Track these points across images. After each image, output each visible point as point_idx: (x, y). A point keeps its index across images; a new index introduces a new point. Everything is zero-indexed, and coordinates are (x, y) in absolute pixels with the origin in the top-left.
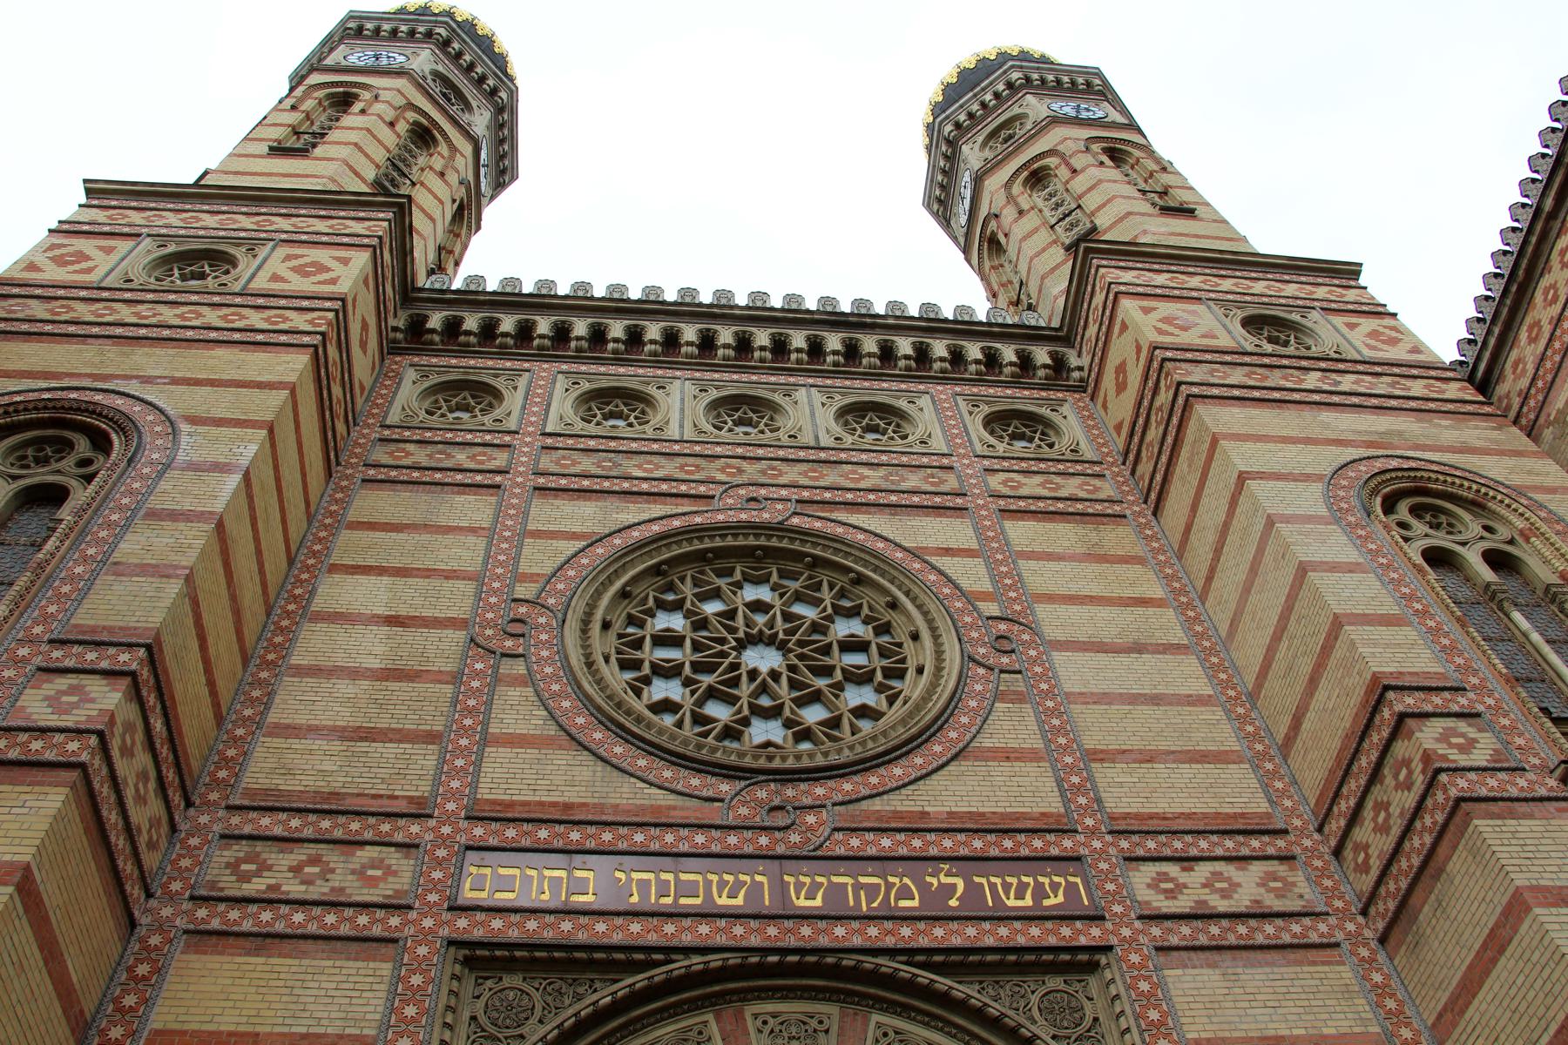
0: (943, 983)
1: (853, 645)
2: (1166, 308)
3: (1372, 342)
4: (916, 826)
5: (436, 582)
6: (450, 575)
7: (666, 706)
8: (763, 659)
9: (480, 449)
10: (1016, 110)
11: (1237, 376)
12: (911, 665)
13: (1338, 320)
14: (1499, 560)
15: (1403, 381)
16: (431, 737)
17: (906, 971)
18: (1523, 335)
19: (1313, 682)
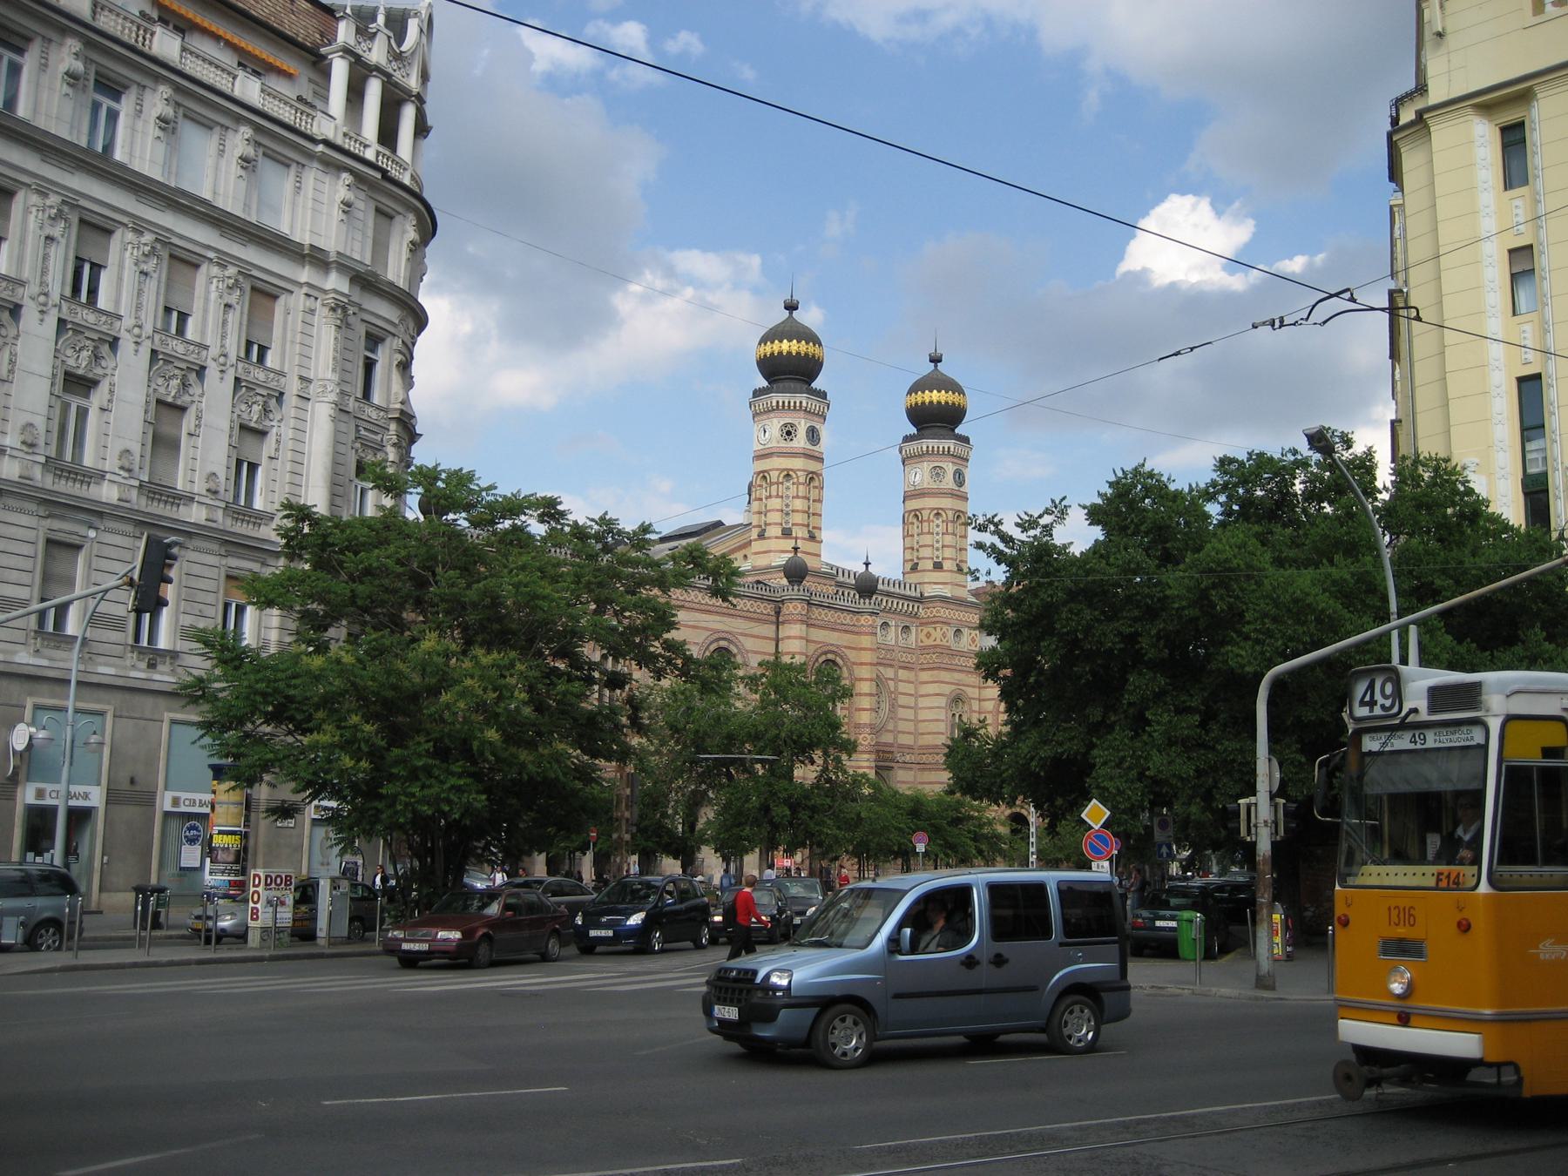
14: (960, 716)
19: (929, 733)
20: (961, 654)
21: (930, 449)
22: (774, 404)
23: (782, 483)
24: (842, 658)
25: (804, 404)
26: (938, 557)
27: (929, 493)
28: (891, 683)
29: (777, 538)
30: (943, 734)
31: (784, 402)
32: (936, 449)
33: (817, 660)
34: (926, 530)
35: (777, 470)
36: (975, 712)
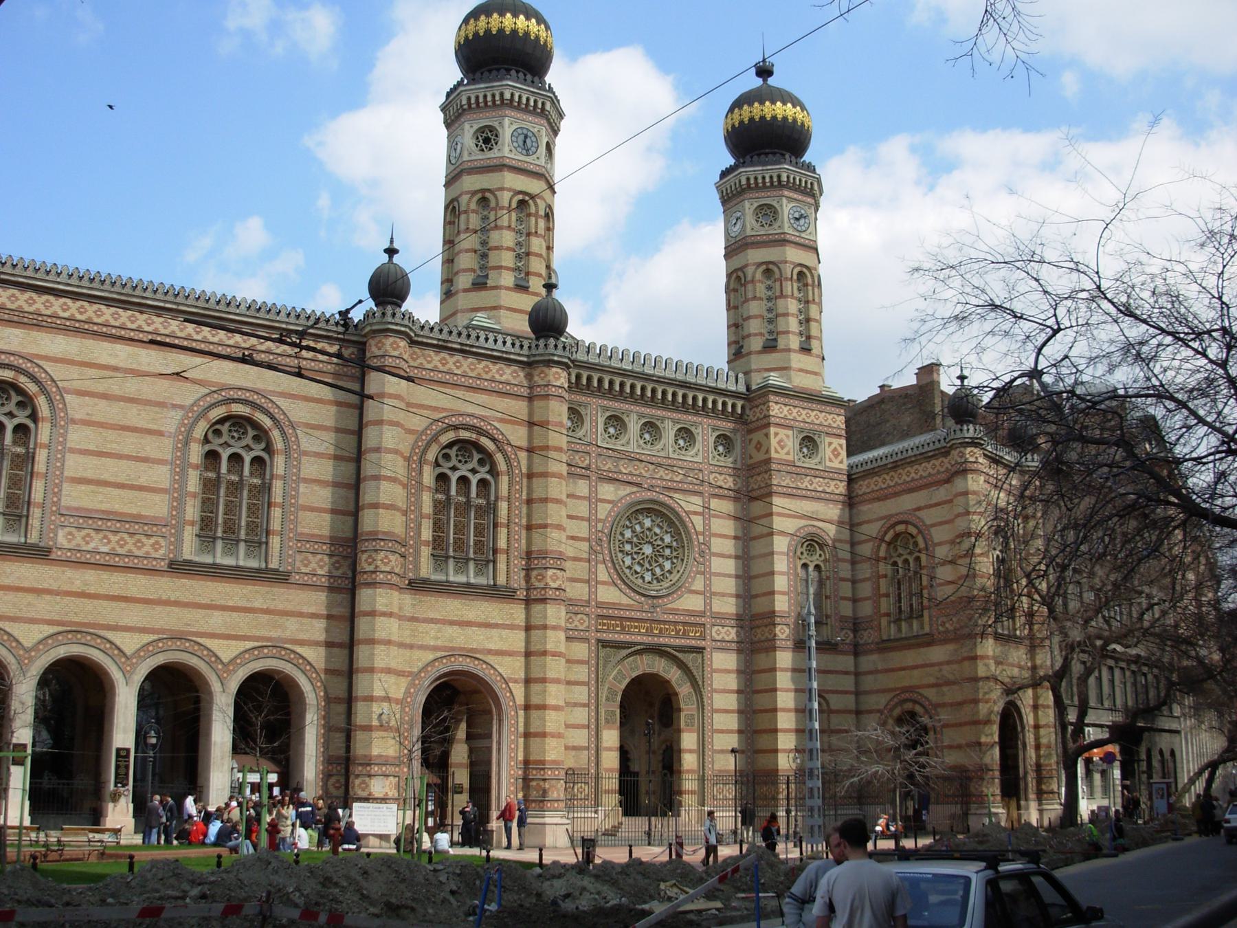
0: (677, 654)
1: (669, 547)
2: (783, 432)
3: (832, 456)
4: (675, 612)
5: (579, 522)
6: (582, 519)
7: (630, 568)
8: (648, 550)
9: (581, 454)
10: (774, 203)
11: (787, 481)
12: (681, 556)
13: (828, 440)
14: (817, 567)
15: (830, 482)
16: (588, 581)
17: (672, 651)
18: (866, 482)
20: (815, 473)
21: (752, 181)
22: (464, 102)
23: (473, 211)
24: (493, 439)
25: (507, 96)
26: (771, 332)
27: (753, 243)
28: (698, 521)
29: (466, 290)
30: (783, 593)
31: (477, 97)
32: (760, 181)
33: (435, 439)
34: (750, 295)
35: (467, 193)
36: (844, 560)
